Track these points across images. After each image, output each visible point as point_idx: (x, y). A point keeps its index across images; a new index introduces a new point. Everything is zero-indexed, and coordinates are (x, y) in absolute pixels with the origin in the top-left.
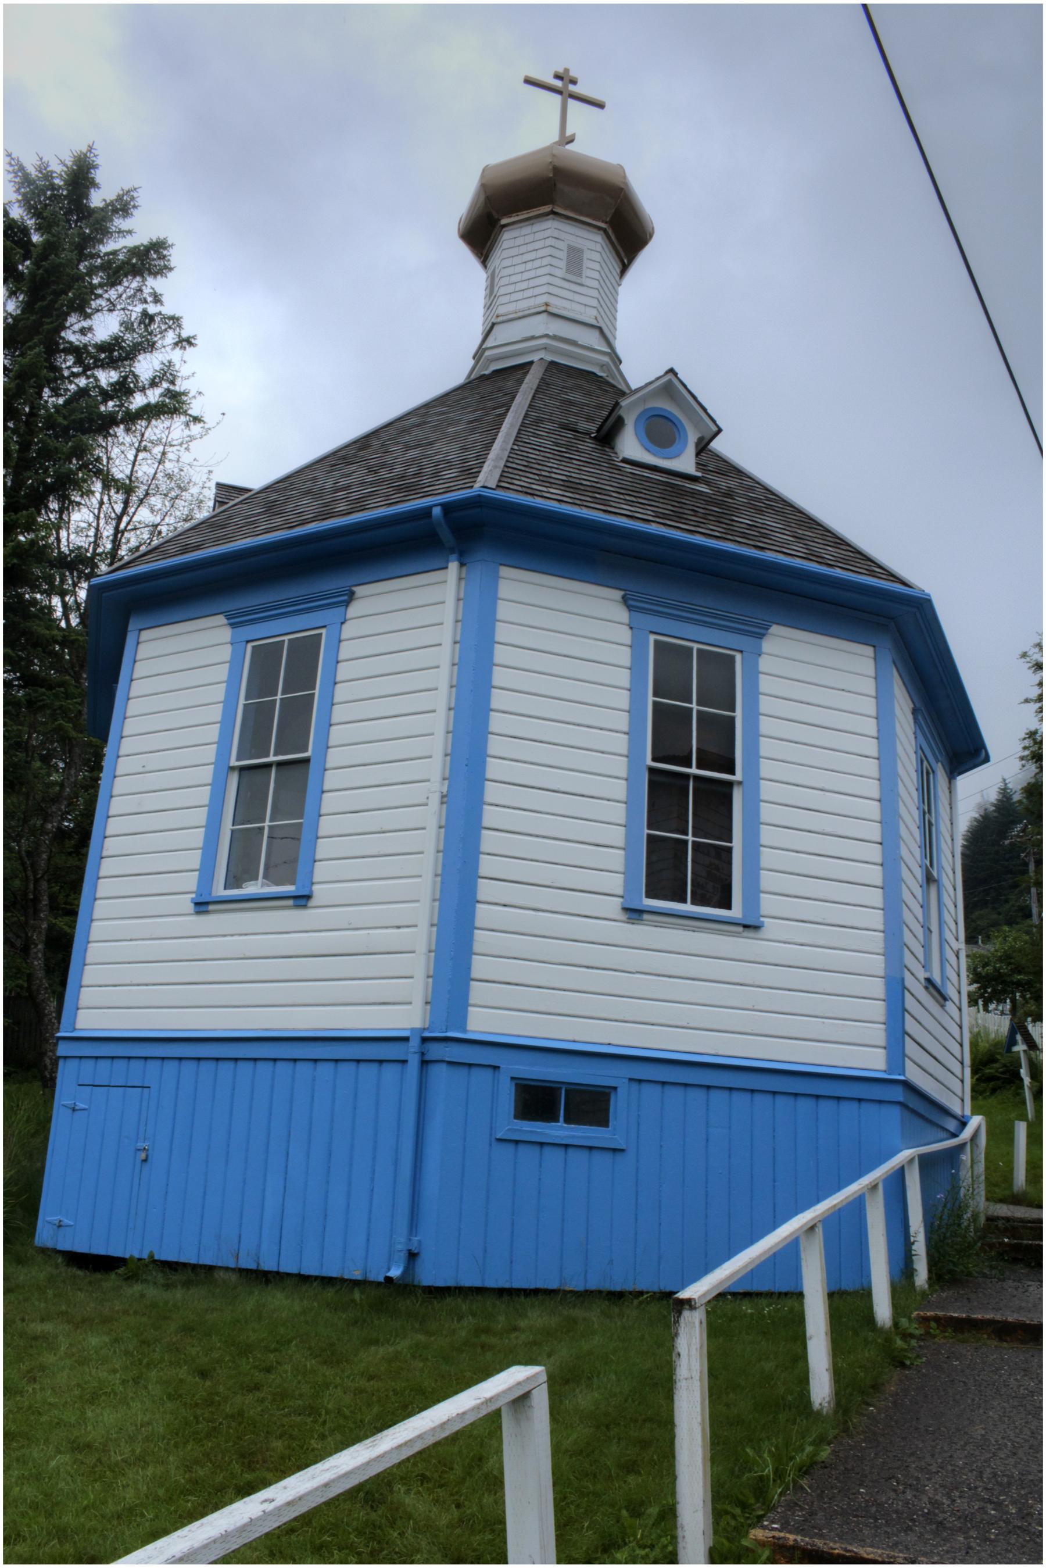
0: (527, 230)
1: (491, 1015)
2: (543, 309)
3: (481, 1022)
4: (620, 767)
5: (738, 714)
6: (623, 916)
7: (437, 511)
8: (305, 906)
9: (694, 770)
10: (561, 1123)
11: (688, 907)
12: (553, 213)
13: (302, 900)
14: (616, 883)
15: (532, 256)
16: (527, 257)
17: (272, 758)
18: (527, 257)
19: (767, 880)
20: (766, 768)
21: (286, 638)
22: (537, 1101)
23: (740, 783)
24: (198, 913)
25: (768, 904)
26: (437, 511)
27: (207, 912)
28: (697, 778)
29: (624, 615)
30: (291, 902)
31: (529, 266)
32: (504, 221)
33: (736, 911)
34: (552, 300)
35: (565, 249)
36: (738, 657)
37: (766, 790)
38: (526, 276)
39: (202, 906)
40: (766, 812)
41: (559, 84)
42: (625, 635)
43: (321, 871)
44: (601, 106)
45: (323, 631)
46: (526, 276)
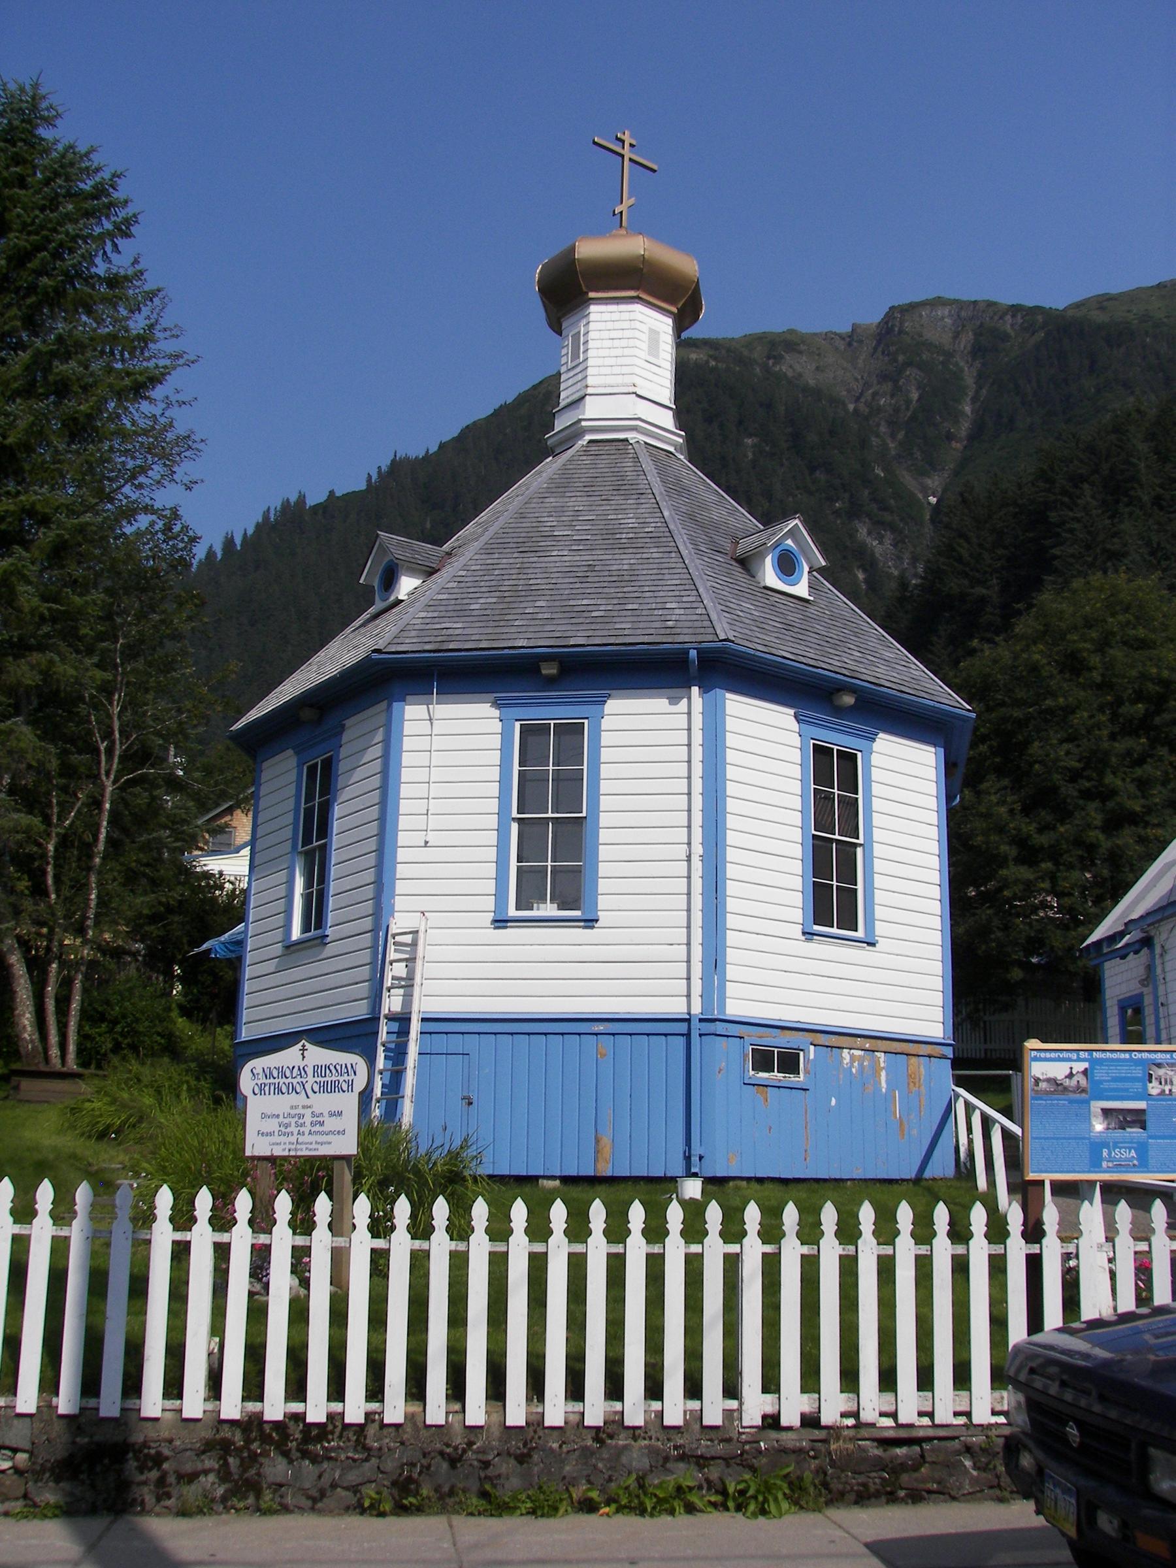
1: (739, 1004)
2: (632, 389)
3: (733, 1009)
4: (797, 834)
5: (860, 796)
7: (693, 654)
8: (592, 927)
9: (837, 837)
10: (776, 1073)
11: (834, 931)
12: (638, 298)
13: (590, 922)
14: (798, 915)
16: (614, 334)
17: (550, 815)
19: (879, 912)
20: (877, 835)
21: (552, 722)
22: (763, 1060)
23: (861, 845)
24: (496, 928)
25: (880, 928)
26: (693, 654)
27: (506, 927)
28: (838, 841)
29: (795, 726)
30: (582, 924)
31: (616, 343)
33: (860, 934)
34: (637, 381)
35: (646, 331)
36: (859, 755)
37: (878, 850)
38: (614, 352)
39: (501, 922)
40: (878, 865)
42: (797, 741)
43: (603, 902)
45: (586, 721)
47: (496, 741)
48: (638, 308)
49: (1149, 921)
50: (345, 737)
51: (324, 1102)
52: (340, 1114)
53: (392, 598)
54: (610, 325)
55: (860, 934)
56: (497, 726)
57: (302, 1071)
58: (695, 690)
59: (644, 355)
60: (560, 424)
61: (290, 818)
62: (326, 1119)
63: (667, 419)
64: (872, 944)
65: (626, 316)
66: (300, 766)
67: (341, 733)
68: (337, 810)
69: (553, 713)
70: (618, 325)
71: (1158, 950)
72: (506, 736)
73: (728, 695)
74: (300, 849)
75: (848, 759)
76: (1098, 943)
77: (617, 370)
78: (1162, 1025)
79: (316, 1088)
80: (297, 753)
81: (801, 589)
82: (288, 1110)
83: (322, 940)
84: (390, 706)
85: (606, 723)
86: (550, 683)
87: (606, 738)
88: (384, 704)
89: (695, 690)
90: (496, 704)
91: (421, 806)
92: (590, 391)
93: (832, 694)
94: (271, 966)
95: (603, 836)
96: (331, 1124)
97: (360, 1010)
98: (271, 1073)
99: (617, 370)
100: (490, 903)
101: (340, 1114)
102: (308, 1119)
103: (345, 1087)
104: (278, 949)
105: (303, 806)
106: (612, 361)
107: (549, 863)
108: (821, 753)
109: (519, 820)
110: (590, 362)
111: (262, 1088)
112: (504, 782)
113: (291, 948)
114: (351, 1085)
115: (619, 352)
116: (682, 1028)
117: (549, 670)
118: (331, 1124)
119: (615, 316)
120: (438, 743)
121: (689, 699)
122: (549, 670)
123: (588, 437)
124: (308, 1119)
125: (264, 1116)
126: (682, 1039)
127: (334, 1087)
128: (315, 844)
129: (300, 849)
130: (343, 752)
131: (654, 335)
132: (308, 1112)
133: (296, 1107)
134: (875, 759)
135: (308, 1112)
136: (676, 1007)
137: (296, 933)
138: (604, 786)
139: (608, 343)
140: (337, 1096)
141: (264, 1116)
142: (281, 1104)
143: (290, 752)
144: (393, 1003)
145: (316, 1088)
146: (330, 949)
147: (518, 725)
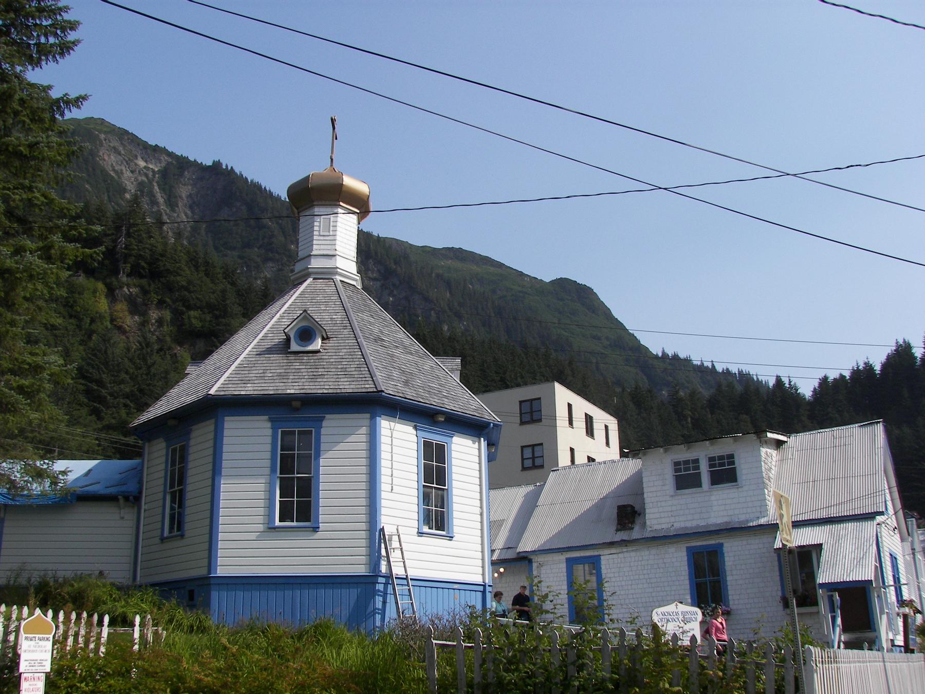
13: (451, 538)
39: (420, 534)
43: (456, 529)
53: (310, 348)
57: (677, 614)
60: (315, 264)
68: (322, 462)
69: (436, 438)
71: (535, 565)
74: (278, 475)
80: (271, 420)
83: (316, 529)
84: (373, 418)
88: (368, 415)
90: (415, 428)
92: (337, 253)
94: (253, 536)
95: (455, 499)
97: (361, 570)
100: (415, 524)
104: (261, 527)
105: (279, 452)
110: (338, 238)
113: (272, 529)
114: (696, 619)
116: (481, 588)
126: (479, 594)
130: (323, 431)
136: (478, 579)
137: (277, 523)
143: (266, 417)
144: (384, 569)
146: (319, 535)
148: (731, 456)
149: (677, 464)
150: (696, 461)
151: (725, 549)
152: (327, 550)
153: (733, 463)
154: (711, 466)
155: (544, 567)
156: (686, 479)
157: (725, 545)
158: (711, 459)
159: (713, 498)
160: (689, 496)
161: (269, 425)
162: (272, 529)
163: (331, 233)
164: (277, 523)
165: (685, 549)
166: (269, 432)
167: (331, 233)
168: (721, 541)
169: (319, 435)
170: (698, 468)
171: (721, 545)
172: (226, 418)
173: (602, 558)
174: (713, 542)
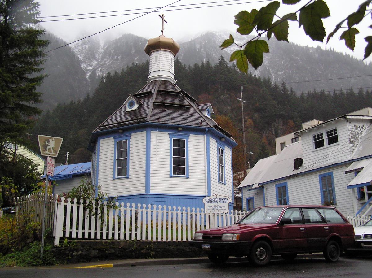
0: (165, 52)
6: (218, 182)
7: (207, 129)
12: (170, 51)
13: (188, 178)
15: (166, 58)
16: (165, 58)
17: (179, 157)
18: (165, 58)
25: (226, 182)
26: (207, 129)
27: (172, 178)
32: (161, 49)
38: (165, 62)
39: (171, 177)
40: (226, 171)
41: (162, 16)
44: (167, 23)
46: (165, 62)
47: (169, 142)
48: (169, 53)
49: (265, 183)
50: (131, 137)
51: (221, 204)
52: (225, 206)
54: (164, 56)
55: (224, 182)
56: (169, 139)
58: (205, 136)
59: (170, 64)
61: (113, 152)
62: (222, 207)
63: (173, 77)
64: (225, 185)
65: (167, 55)
66: (115, 142)
67: (130, 136)
70: (166, 56)
71: (265, 189)
72: (170, 141)
73: (210, 137)
75: (222, 150)
76: (242, 188)
77: (166, 66)
78: (266, 202)
79: (220, 202)
81: (210, 117)
82: (214, 206)
83: (128, 178)
85: (189, 140)
86: (179, 131)
87: (189, 143)
88: (146, 132)
89: (205, 136)
91: (155, 153)
93: (221, 138)
96: (223, 208)
98: (210, 200)
99: (166, 66)
101: (225, 206)
102: (218, 207)
103: (226, 202)
106: (165, 64)
107: (179, 166)
108: (219, 149)
109: (173, 157)
111: (208, 202)
112: (170, 150)
114: (227, 202)
115: (166, 62)
117: (180, 129)
118: (223, 208)
119: (165, 54)
120: (158, 141)
121: (204, 137)
122: (180, 129)
123: (161, 79)
124: (218, 207)
125: (209, 207)
127: (224, 202)
128: (122, 158)
129: (116, 159)
130: (131, 140)
131: (172, 59)
132: (218, 206)
133: (216, 205)
134: (225, 151)
135: (218, 206)
137: (116, 177)
138: (189, 152)
139: (164, 60)
140: (224, 203)
141: (209, 207)
142: (213, 205)
145: (220, 202)
147: (173, 139)
148: (335, 130)
149: (315, 137)
150: (322, 134)
151: (334, 175)
152: (133, 185)
153: (336, 133)
154: (328, 136)
155: (268, 189)
156: (319, 144)
157: (334, 172)
158: (328, 132)
159: (329, 151)
160: (321, 151)
161: (113, 140)
162: (114, 179)
163: (158, 62)
164: (116, 177)
165: (318, 176)
166: (114, 143)
167: (158, 62)
168: (332, 171)
169: (129, 142)
170: (322, 137)
171: (333, 172)
172: (101, 140)
173: (288, 183)
174: (329, 172)
